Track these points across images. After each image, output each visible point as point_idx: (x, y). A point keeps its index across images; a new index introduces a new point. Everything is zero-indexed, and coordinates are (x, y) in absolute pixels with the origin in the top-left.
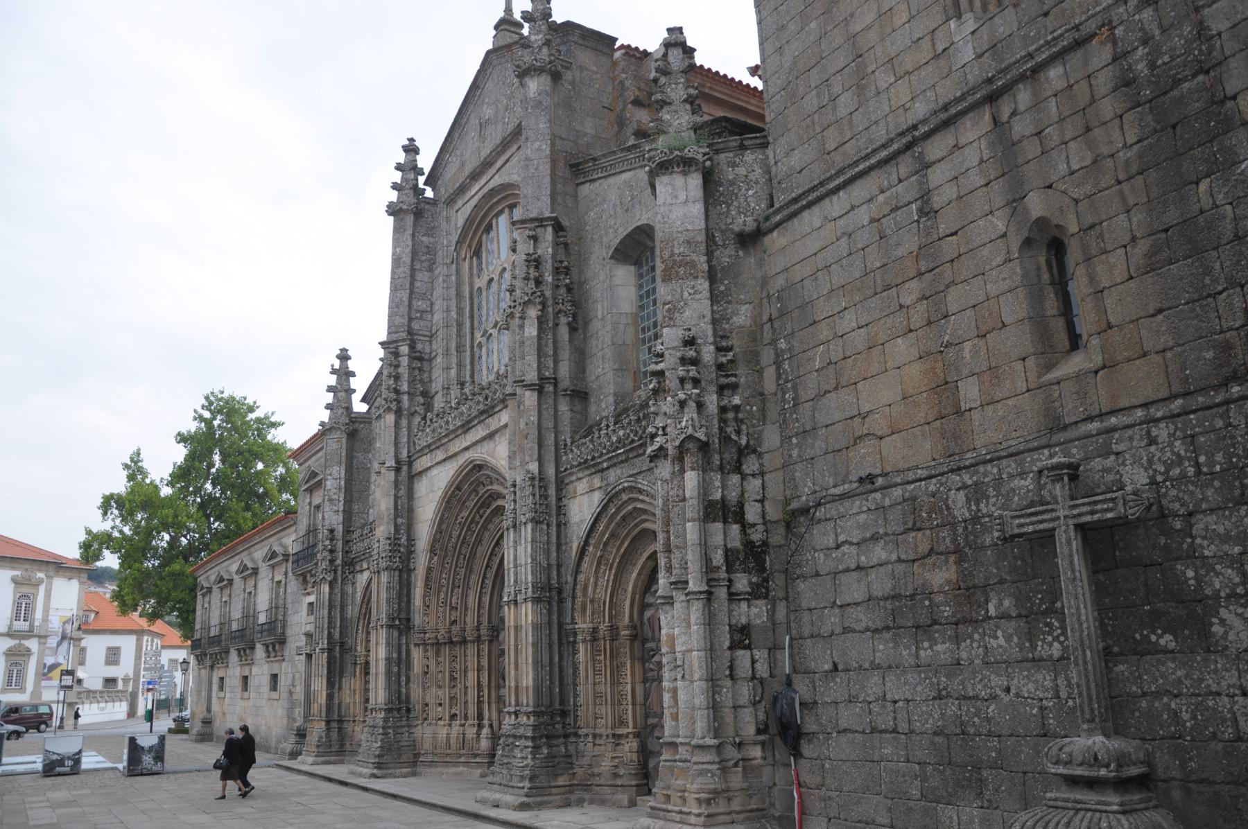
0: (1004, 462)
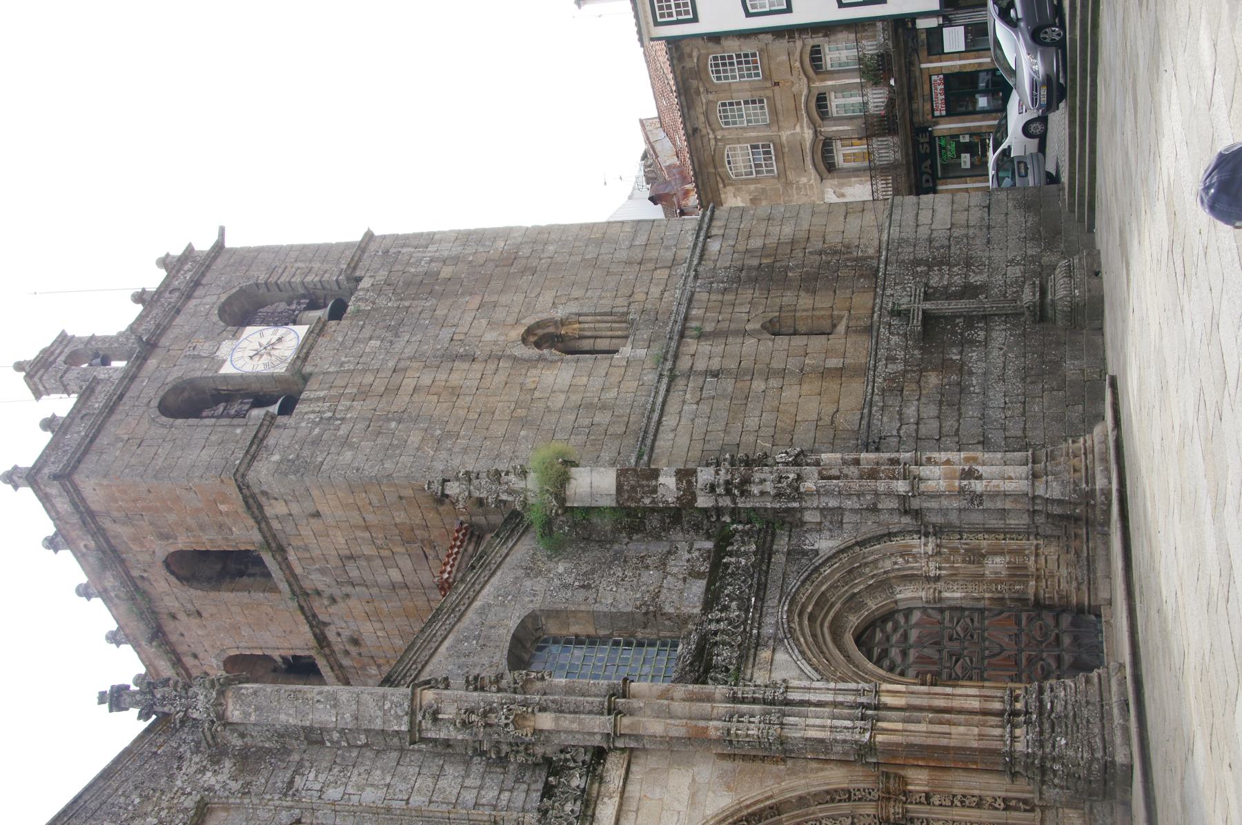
0: (879, 346)
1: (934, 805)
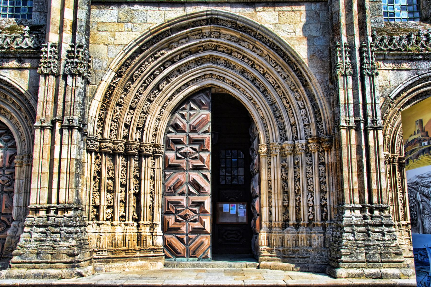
1: (319, 167)
